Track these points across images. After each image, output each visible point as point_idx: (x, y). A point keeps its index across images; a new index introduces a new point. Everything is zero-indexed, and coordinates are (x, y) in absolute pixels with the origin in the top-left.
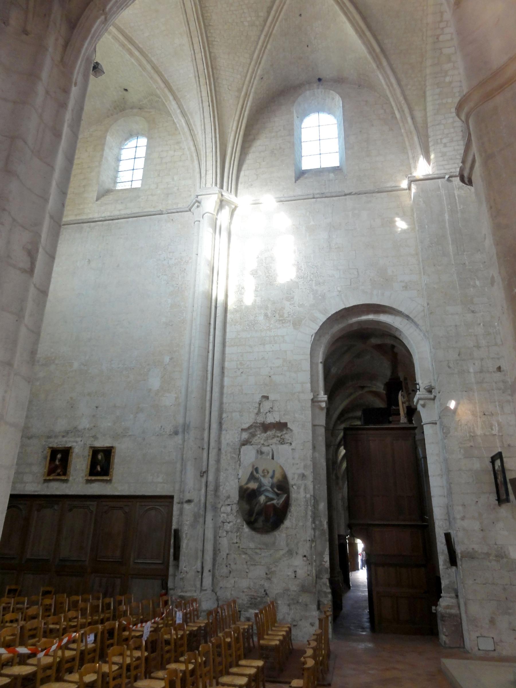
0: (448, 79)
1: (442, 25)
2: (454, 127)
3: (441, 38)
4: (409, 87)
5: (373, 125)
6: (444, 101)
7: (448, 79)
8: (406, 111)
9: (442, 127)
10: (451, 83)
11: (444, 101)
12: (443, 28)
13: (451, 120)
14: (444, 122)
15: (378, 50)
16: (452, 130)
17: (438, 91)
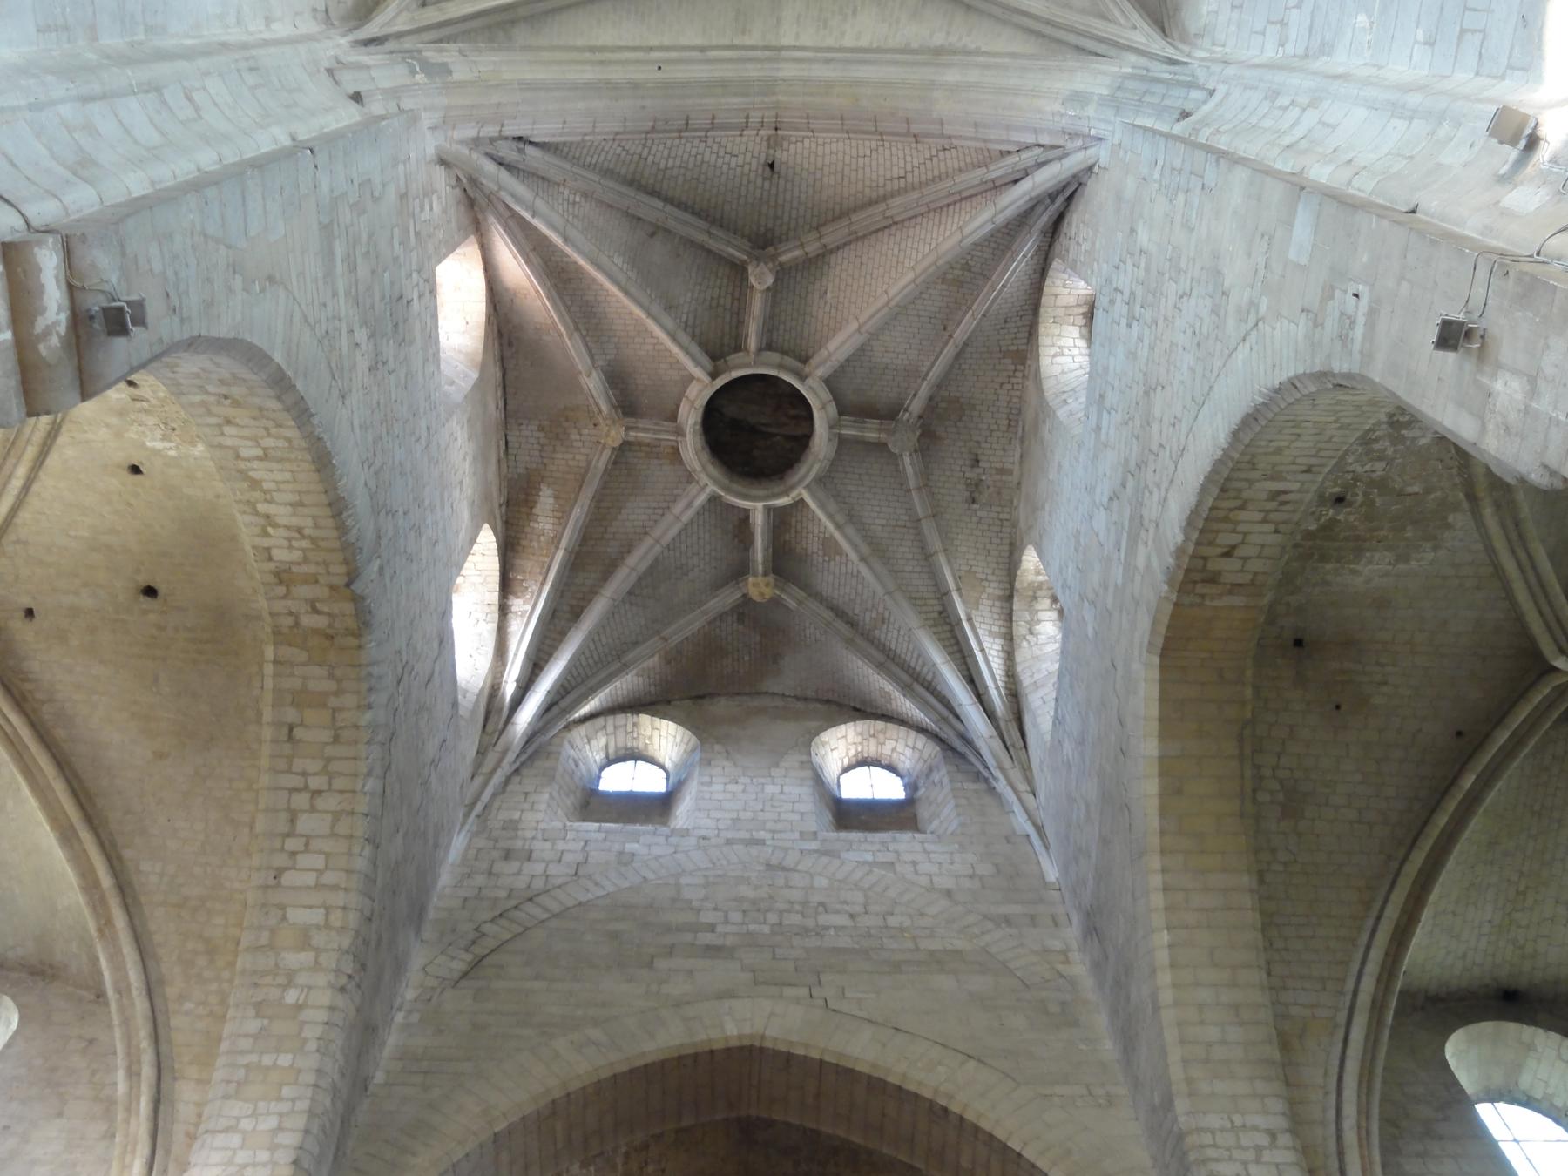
0: (292, 996)
1: (291, 844)
2: (273, 1148)
3: (288, 879)
4: (188, 1006)
5: (60, 1115)
6: (267, 1060)
7: (292, 996)
8: (147, 1071)
9: (236, 1140)
10: (299, 1007)
11: (267, 1060)
12: (293, 854)
13: (272, 1122)
14: (246, 1124)
15: (106, 881)
16: (264, 1156)
17: (253, 1025)
